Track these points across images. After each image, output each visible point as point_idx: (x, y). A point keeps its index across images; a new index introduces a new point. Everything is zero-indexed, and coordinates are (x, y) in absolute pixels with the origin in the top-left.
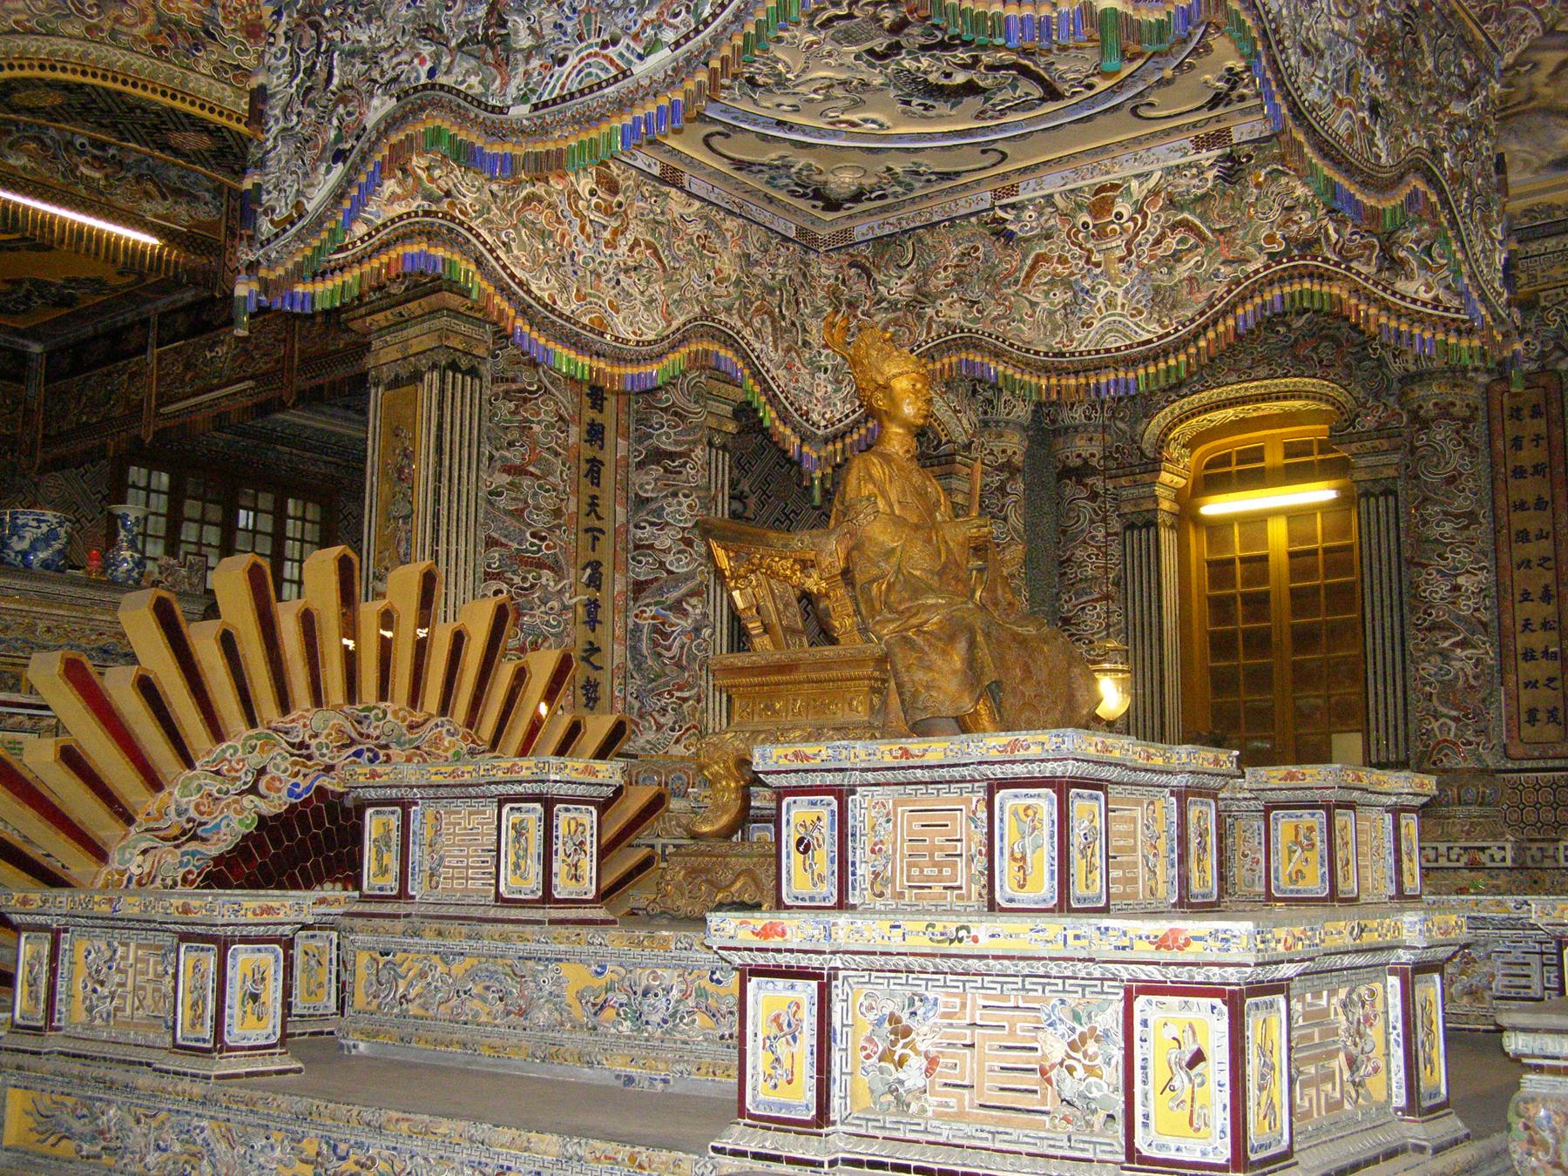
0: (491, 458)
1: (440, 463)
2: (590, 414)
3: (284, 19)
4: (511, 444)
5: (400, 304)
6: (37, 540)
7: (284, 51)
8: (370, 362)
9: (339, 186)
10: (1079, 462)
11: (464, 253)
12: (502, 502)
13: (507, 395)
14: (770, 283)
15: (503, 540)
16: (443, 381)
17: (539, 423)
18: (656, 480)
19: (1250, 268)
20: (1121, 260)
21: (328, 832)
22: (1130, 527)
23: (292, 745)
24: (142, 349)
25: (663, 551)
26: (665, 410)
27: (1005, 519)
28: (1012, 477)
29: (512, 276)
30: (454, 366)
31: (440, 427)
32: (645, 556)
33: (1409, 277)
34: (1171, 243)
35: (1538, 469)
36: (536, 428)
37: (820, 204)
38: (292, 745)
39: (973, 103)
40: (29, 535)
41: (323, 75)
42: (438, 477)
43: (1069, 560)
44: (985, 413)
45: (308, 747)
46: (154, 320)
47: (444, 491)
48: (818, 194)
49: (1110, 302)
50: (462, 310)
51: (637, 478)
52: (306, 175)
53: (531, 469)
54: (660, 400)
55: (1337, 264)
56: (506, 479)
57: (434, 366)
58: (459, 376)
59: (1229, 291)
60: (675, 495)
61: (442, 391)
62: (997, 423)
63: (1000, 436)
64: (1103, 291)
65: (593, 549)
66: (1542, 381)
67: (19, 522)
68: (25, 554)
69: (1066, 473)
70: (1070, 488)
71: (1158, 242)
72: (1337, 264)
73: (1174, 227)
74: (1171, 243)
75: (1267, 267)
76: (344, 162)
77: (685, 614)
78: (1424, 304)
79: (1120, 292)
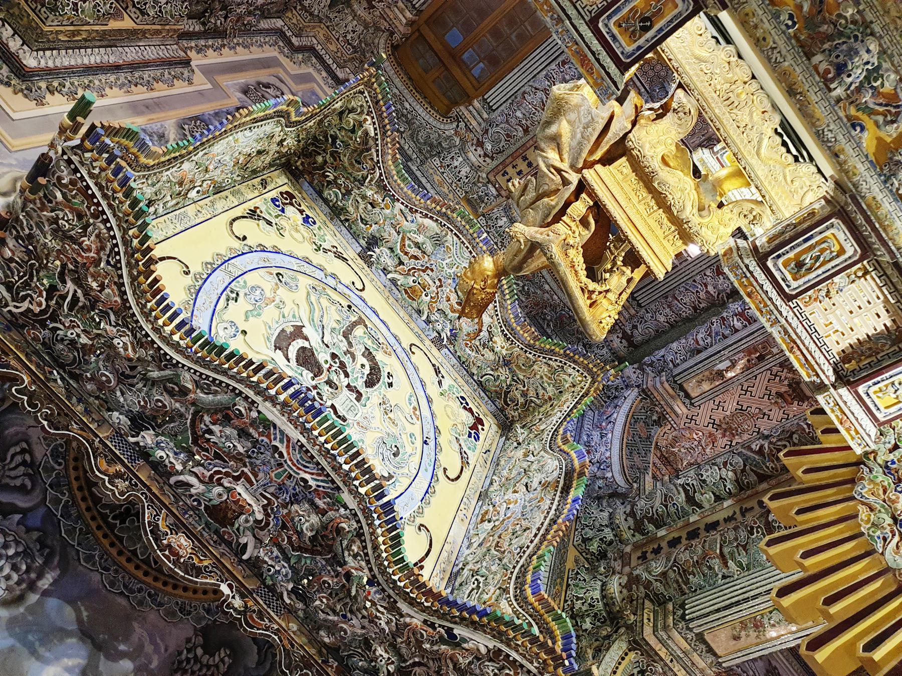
0: (724, 577)
1: (738, 603)
2: (684, 541)
4: (710, 568)
5: (666, 664)
9: (467, 626)
10: (623, 341)
11: (529, 565)
12: (744, 561)
13: (687, 582)
14: (526, 433)
16: (692, 620)
17: (692, 558)
18: (702, 494)
19: (403, 207)
20: (432, 270)
22: (639, 305)
25: (736, 474)
26: (666, 506)
27: (663, 356)
28: (645, 364)
29: (536, 535)
30: (683, 617)
31: (718, 610)
32: (743, 482)
33: (366, 133)
34: (413, 251)
35: (525, 158)
36: (695, 558)
37: (480, 427)
39: (379, 357)
42: (746, 600)
43: (667, 322)
44: (622, 389)
47: (752, 593)
48: (474, 427)
49: (451, 266)
50: (651, 625)
51: (707, 506)
52: (478, 659)
53: (718, 551)
55: (380, 169)
56: (731, 563)
57: (691, 630)
58: (687, 612)
59: (416, 211)
60: (704, 481)
61: (698, 618)
62: (624, 381)
63: (628, 377)
64: (449, 271)
65: (753, 508)
66: (492, 179)
69: (631, 344)
70: (638, 338)
71: (416, 258)
72: (380, 169)
73: (406, 254)
74: (413, 251)
75: (398, 200)
76: (452, 629)
77: (762, 446)
78: (373, 118)
79: (444, 263)
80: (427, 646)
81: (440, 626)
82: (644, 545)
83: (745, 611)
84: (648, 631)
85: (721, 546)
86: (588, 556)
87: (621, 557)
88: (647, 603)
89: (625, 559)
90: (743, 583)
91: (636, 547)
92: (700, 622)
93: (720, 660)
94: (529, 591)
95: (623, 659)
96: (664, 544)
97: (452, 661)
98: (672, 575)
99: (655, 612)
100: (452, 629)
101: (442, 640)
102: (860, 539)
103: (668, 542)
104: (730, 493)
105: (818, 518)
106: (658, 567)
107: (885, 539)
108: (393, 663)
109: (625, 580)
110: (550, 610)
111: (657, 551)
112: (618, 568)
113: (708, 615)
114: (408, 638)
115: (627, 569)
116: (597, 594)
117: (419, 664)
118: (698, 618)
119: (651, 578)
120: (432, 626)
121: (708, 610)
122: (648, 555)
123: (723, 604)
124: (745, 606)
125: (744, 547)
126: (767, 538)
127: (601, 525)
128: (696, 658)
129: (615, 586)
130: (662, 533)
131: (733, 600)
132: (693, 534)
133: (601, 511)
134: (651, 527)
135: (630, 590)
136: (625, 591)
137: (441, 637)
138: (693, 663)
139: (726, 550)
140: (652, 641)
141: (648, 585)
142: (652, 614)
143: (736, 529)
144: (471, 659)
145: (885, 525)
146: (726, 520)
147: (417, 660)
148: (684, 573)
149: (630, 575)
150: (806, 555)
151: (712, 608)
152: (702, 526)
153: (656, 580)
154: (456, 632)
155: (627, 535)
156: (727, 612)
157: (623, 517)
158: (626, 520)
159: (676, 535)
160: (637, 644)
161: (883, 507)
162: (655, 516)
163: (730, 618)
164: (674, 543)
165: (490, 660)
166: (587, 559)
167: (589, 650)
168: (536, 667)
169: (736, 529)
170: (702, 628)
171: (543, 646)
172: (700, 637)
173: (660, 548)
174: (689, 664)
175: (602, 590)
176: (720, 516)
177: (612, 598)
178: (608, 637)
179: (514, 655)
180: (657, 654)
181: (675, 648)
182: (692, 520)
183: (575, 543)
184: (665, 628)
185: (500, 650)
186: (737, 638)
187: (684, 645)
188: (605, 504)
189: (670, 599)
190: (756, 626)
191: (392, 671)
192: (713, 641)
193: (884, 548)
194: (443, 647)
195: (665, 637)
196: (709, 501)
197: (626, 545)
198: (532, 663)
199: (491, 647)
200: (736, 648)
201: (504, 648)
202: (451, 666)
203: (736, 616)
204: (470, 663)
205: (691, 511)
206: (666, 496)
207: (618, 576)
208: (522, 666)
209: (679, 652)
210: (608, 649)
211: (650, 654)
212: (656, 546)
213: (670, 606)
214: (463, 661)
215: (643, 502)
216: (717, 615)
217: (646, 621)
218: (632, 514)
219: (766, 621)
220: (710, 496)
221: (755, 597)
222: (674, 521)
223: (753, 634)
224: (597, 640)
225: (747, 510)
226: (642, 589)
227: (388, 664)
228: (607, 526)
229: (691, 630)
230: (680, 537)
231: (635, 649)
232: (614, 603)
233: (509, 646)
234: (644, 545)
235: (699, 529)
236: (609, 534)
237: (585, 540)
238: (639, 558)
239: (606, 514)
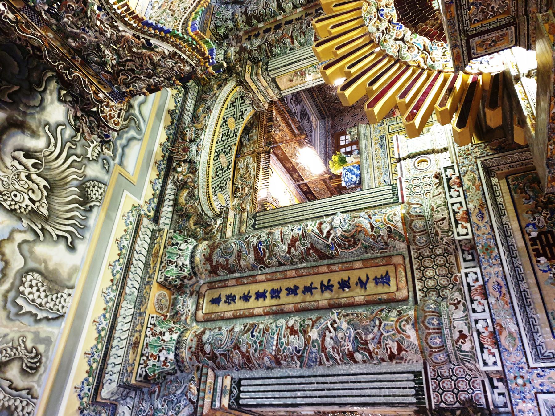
0: (291, 49)
1: (295, 62)
2: (272, 31)
3: (124, 90)
4: (284, 44)
5: (255, 93)
6: (352, 174)
7: (134, 86)
8: (275, 99)
9: (158, 39)
12: (302, 40)
13: (271, 51)
15: (314, 35)
17: (276, 38)
21: (412, 14)
23: (383, 35)
24: (306, 184)
30: (266, 69)
31: (285, 66)
36: (277, 38)
38: (383, 35)
40: (350, 176)
41: (129, 63)
42: (300, 61)
45: (383, 30)
46: (297, 183)
47: (303, 57)
51: (288, 10)
52: (163, 58)
53: (290, 35)
54: (263, 12)
56: (295, 42)
57: (269, 76)
61: (274, 69)
65: (312, 13)
67: (348, 180)
68: (357, 176)
76: (149, 40)
80: (135, 50)
81: (143, 38)
82: (250, 32)
83: (297, 67)
84: (247, 76)
85: (292, 32)
86: (218, 37)
87: (237, 38)
88: (249, 62)
89: (238, 39)
90: (300, 53)
91: (246, 32)
92: (275, 72)
93: (281, 92)
94: (190, 30)
95: (233, 90)
96: (261, 32)
97: (149, 58)
98: (264, 47)
99: (252, 67)
100: (149, 40)
101: (143, 47)
102: (360, 19)
103: (264, 31)
104: (302, 4)
105: (343, 9)
106: (257, 42)
107: (371, 19)
108: (115, 59)
109: (237, 49)
110: (202, 39)
111: (257, 36)
112: (234, 44)
113: (279, 68)
114: (124, 44)
115: (239, 44)
116: (221, 57)
117: (130, 60)
118: (274, 69)
119: (252, 49)
120: (138, 37)
121: (280, 66)
122: (252, 37)
123: (288, 63)
124: (299, 64)
125: (304, 33)
126: (317, 19)
127: (227, 19)
128: (270, 91)
129: (232, 52)
130: (261, 25)
131: (293, 61)
132: (278, 27)
133: (227, 10)
134: (255, 22)
135: (240, 54)
136: (237, 55)
137: (143, 44)
138: (268, 94)
139: (294, 34)
140: (249, 81)
141: (250, 52)
142: (250, 68)
143: (301, 23)
144: (160, 57)
145: (373, 12)
146: (297, 20)
147: (129, 58)
148: (270, 46)
149: (241, 46)
150: (333, 27)
151: (282, 65)
152: (284, 22)
153: (255, 50)
154: (152, 42)
155: (241, 26)
156: (289, 67)
157: (240, 15)
158: (241, 16)
159: (268, 27)
160: (241, 82)
161: (374, 3)
162: (259, 15)
163: (290, 70)
164: (267, 31)
165: (170, 58)
166: (217, 39)
167: (215, 86)
168: (195, 63)
169: (301, 23)
170: (276, 75)
171: (199, 51)
172: (274, 80)
173: (259, 34)
174: (266, 94)
175: (225, 55)
176: (294, 17)
177: (230, 59)
178: (226, 79)
179: (183, 56)
180: (251, 88)
181: (260, 85)
182: (279, 18)
183: (211, 28)
184: (257, 75)
185: (176, 53)
186: (291, 80)
187: (265, 83)
188: (230, 7)
189: (261, 60)
190: (302, 75)
191: (114, 64)
192: (280, 82)
193: (369, 23)
194: (144, 51)
195: (256, 79)
196: (290, 8)
197: (240, 32)
198: (192, 60)
199: (171, 51)
200: (290, 86)
201: (178, 51)
202: (149, 61)
203: (293, 69)
204: (159, 60)
205: (279, 13)
206: (266, 3)
207: (234, 48)
208: (187, 62)
209: (262, 88)
210: (225, 85)
211: (248, 88)
212: (257, 33)
213: (261, 64)
214: (156, 59)
215: (252, 6)
216: (283, 69)
217: (247, 71)
218: (245, 13)
219: (307, 72)
220: (290, 5)
221: (303, 59)
222: (268, 19)
223: (299, 79)
224: (220, 81)
225: (309, 14)
226: (247, 54)
227: (112, 60)
228: (230, 19)
229: (269, 76)
230: (271, 28)
231: (239, 85)
232: (230, 62)
233: (181, 51)
234: (250, 32)
235: (281, 24)
236: (230, 24)
237: (217, 27)
238: (246, 39)
239: (230, 13)
